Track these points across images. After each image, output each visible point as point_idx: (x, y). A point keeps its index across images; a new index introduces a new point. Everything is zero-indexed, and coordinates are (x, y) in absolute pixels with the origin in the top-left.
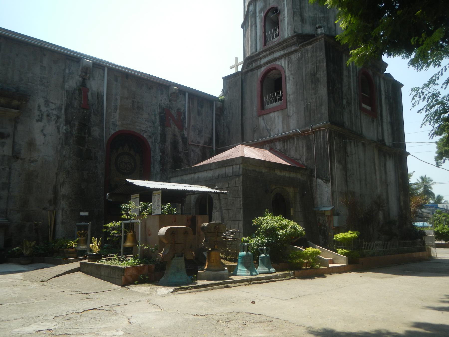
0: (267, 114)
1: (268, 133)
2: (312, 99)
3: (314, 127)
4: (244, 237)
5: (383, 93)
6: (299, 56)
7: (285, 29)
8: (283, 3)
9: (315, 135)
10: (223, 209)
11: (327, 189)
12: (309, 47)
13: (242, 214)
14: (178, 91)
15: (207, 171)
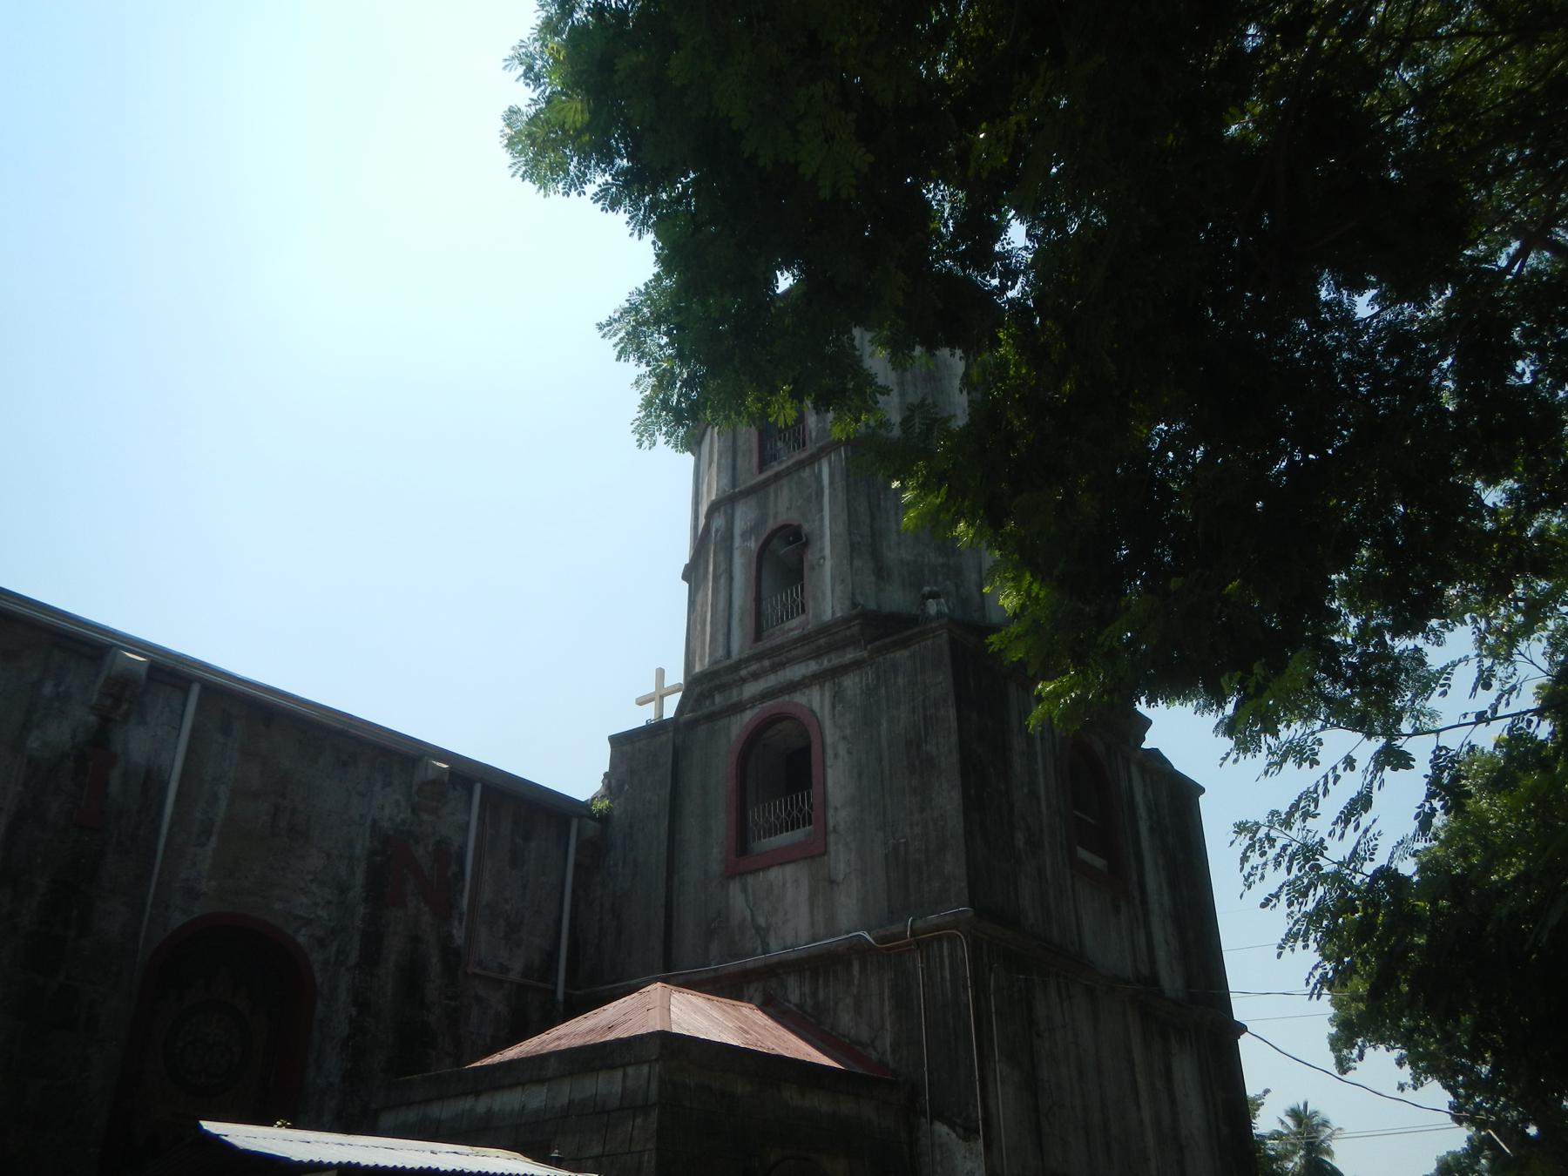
0: (757, 870)
1: (759, 942)
3: (919, 924)
5: (1142, 811)
6: (867, 680)
7: (824, 594)
8: (818, 516)
9: (924, 954)
11: (969, 1165)
12: (901, 655)
14: (446, 778)
15: (523, 1085)
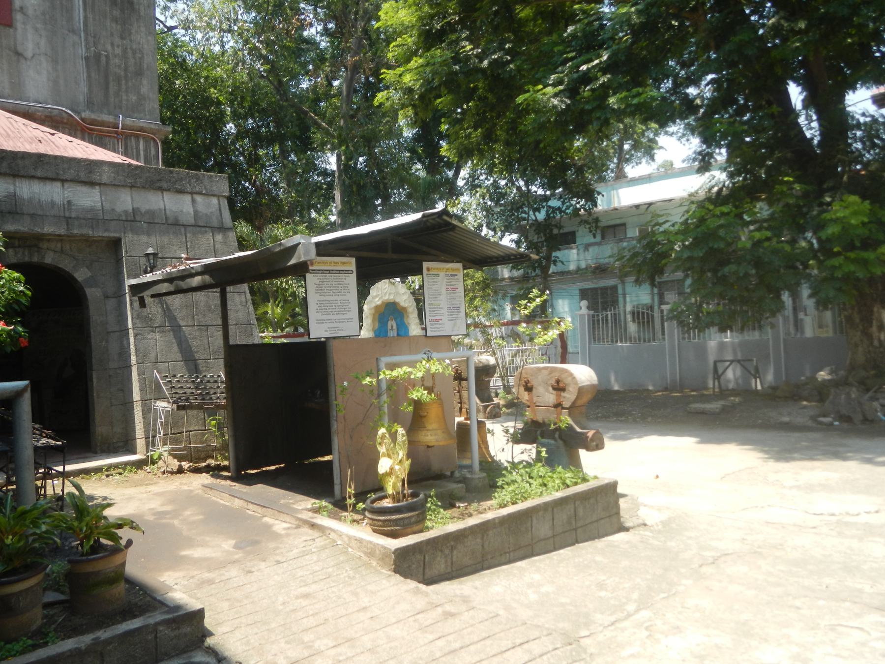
2: (112, 45)
3: (129, 121)
10: (182, 324)
15: (63, 181)
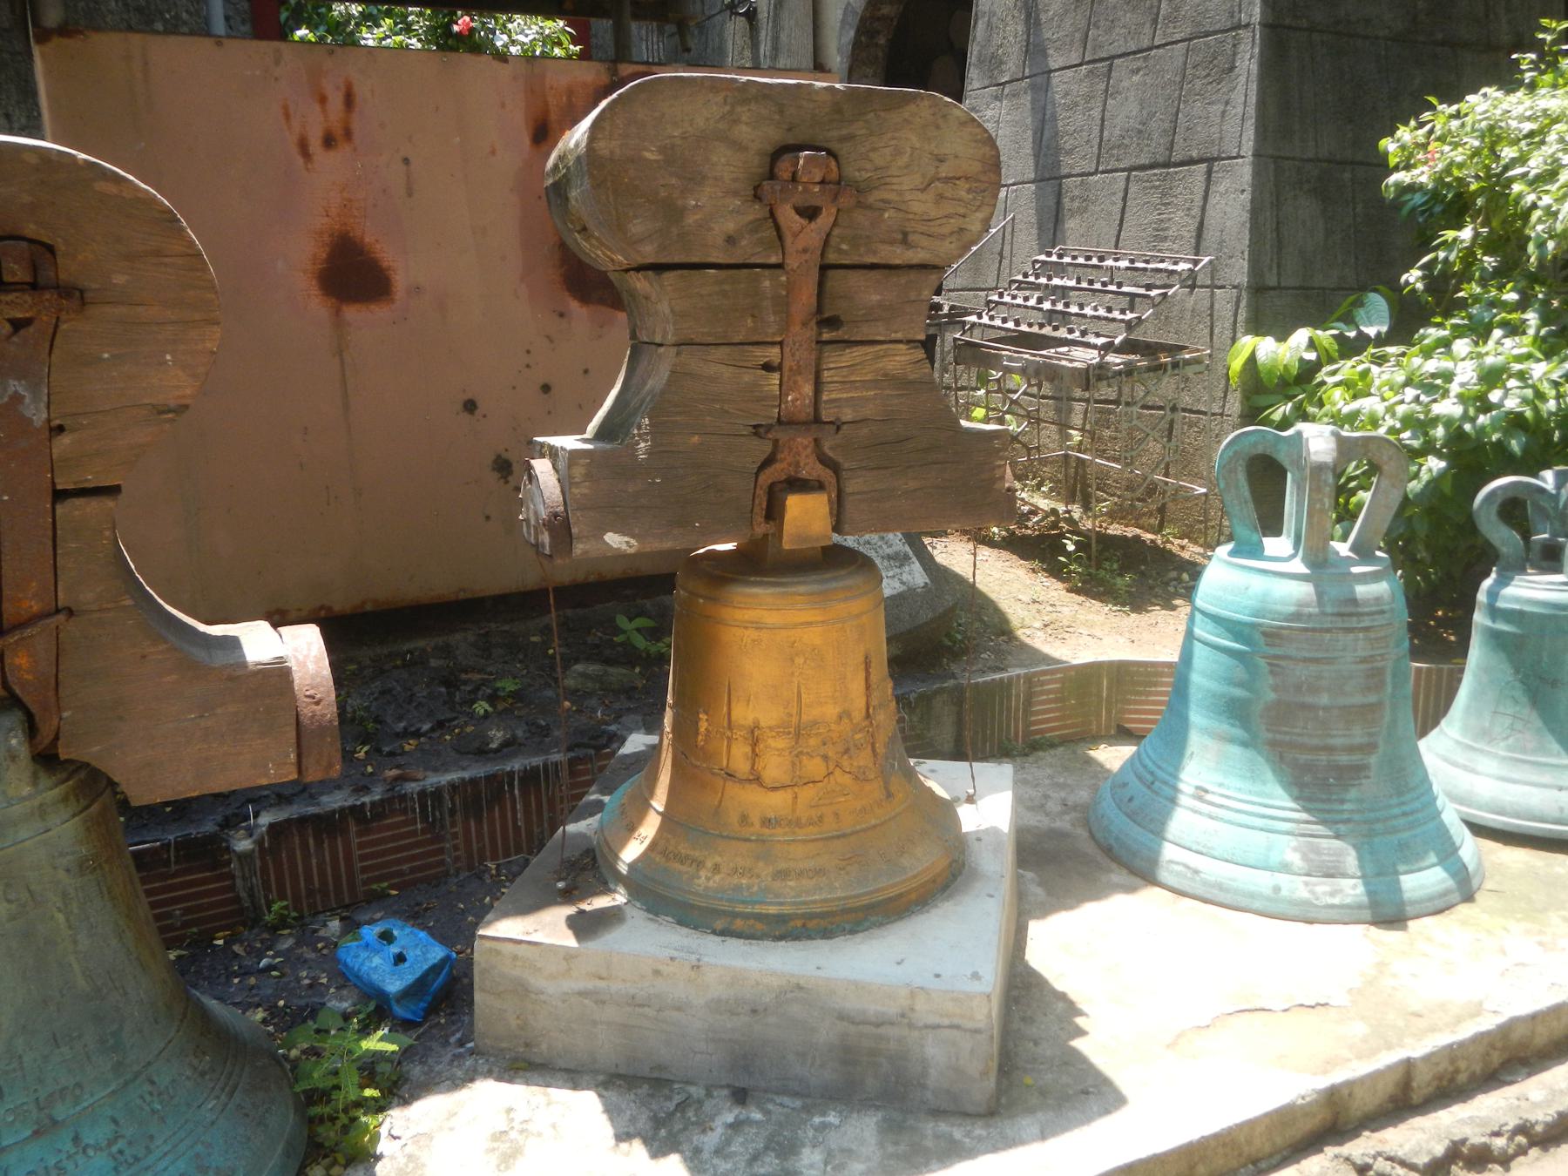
4: (1258, 327)
10: (1053, 65)
13: (1254, 87)
